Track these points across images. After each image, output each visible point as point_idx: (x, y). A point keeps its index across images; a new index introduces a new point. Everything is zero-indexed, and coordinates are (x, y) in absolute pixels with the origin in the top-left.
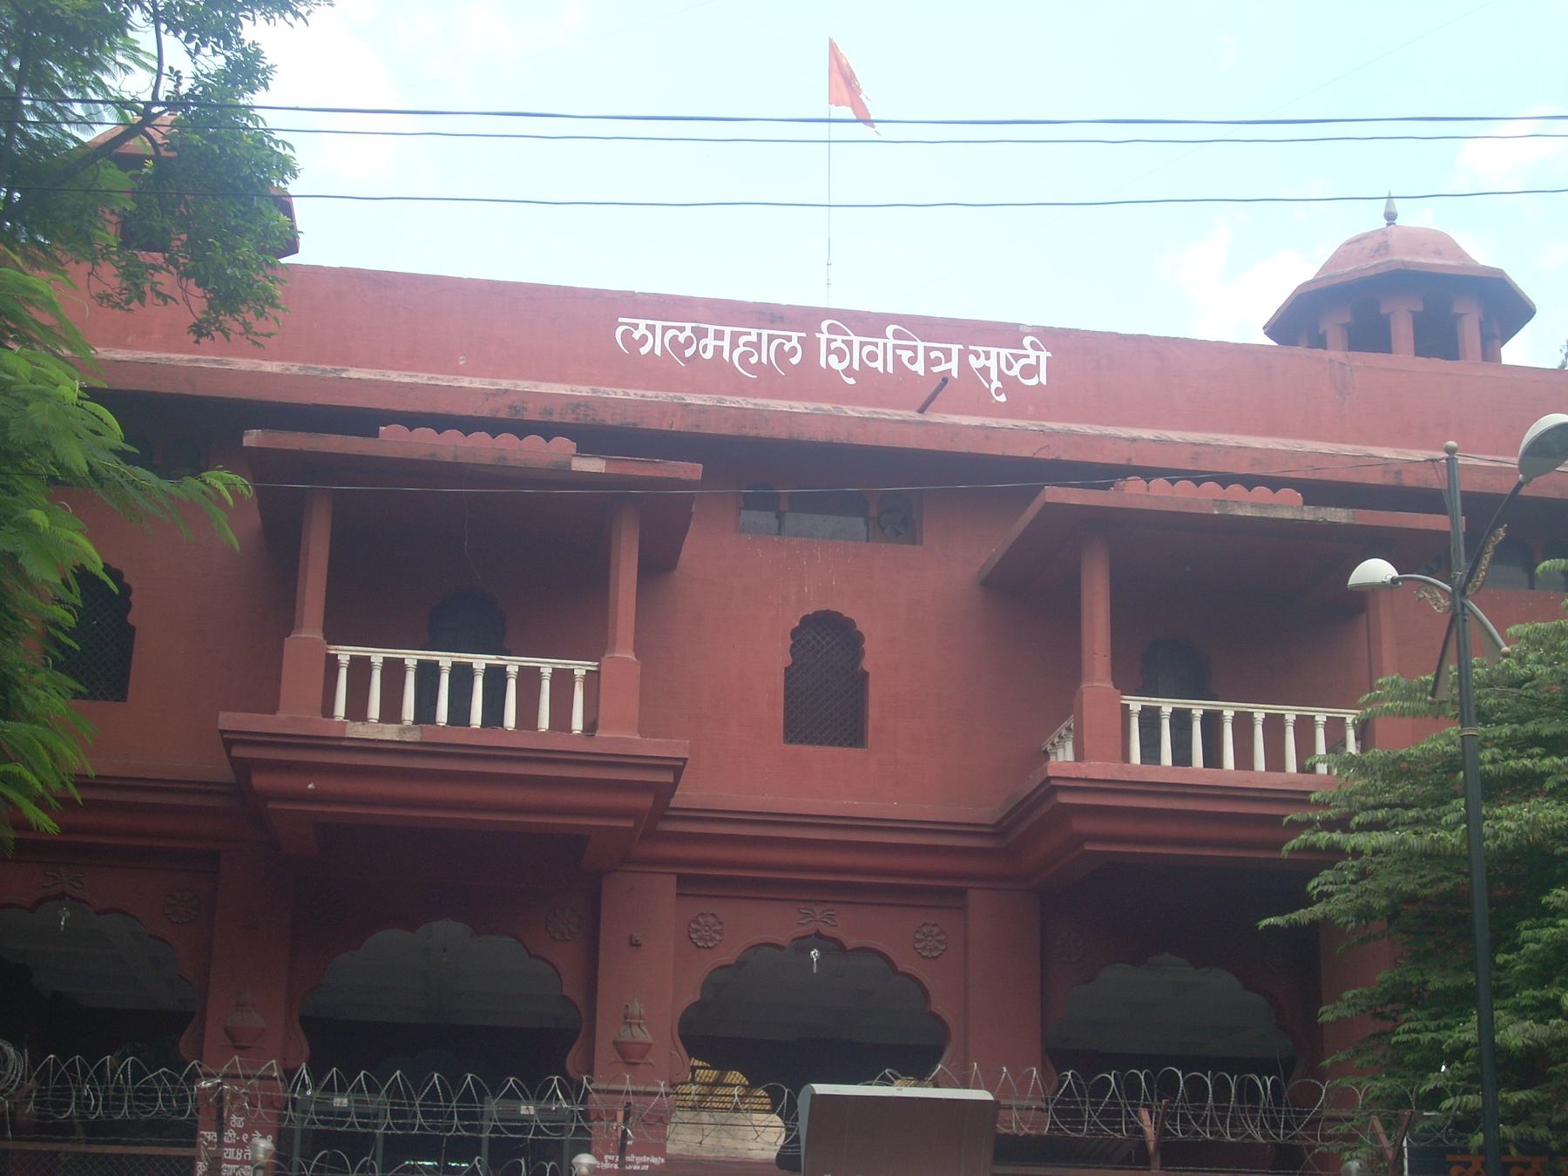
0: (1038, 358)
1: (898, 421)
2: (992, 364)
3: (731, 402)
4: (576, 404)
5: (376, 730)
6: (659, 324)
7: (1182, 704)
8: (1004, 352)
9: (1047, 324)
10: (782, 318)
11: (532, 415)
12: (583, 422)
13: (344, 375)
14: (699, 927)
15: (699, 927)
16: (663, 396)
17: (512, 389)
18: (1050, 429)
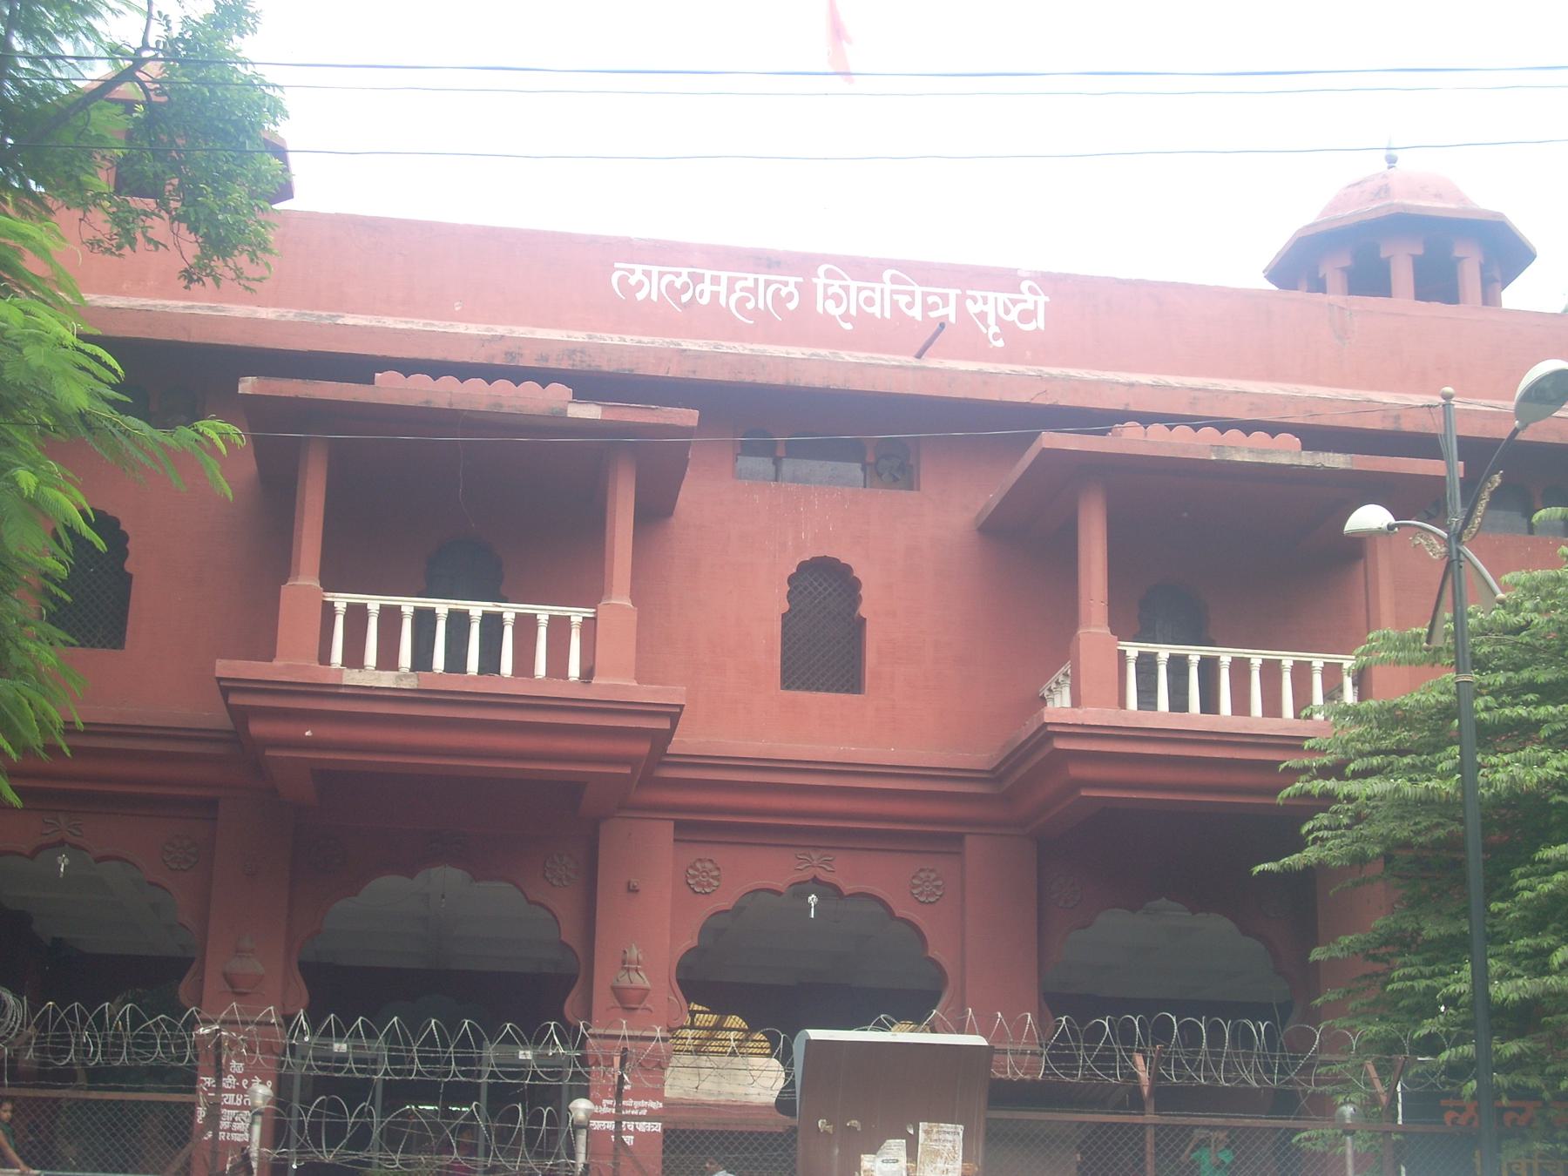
0: (1036, 302)
1: (898, 367)
2: (990, 309)
3: (727, 347)
4: (572, 350)
5: (373, 678)
6: (655, 270)
7: (1179, 650)
8: (1003, 297)
9: (1046, 269)
10: (778, 263)
11: (528, 361)
12: (579, 368)
13: (339, 322)
14: (696, 873)
15: (696, 873)
16: (659, 342)
17: (508, 335)
18: (1047, 374)
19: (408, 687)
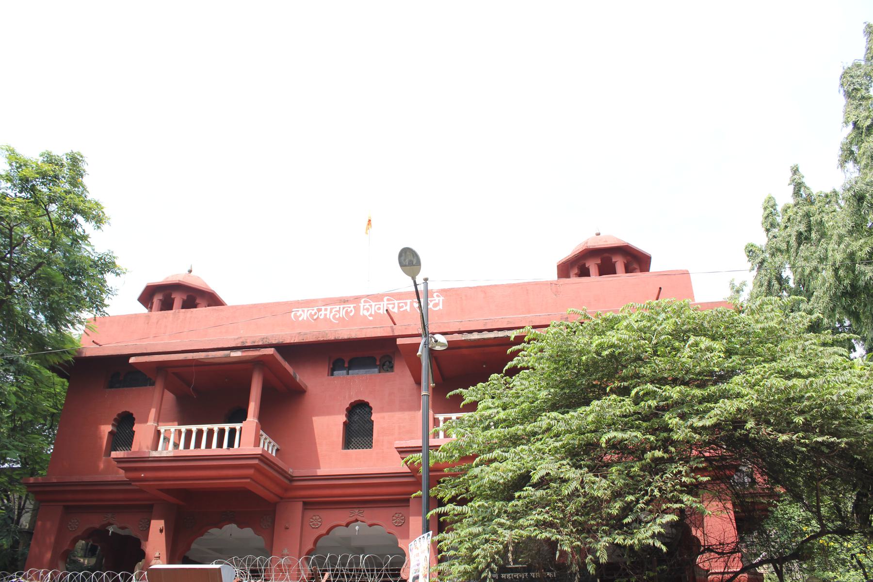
6: (306, 309)
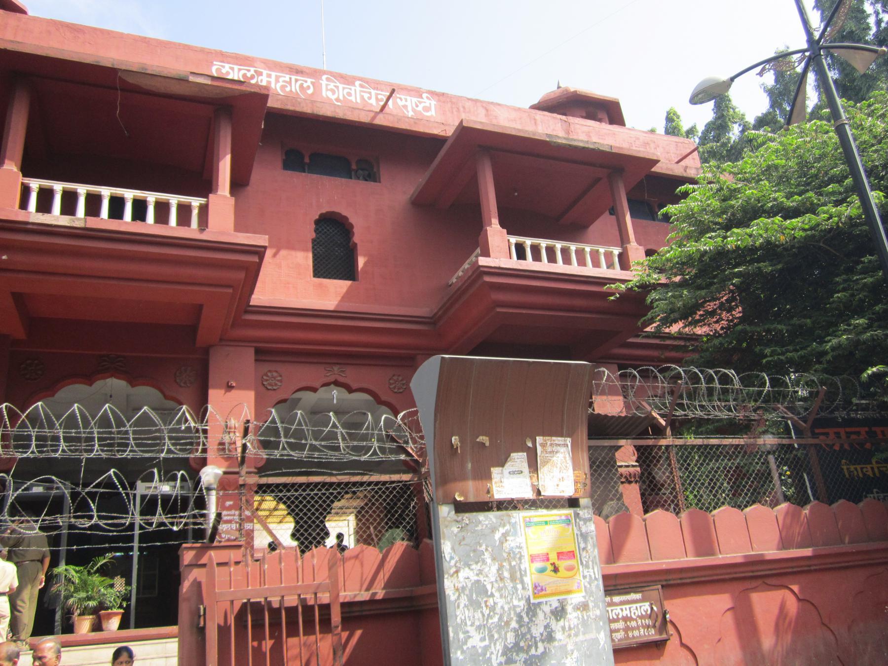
2: (408, 104)
6: (236, 67)
8: (415, 100)
19: (78, 226)
